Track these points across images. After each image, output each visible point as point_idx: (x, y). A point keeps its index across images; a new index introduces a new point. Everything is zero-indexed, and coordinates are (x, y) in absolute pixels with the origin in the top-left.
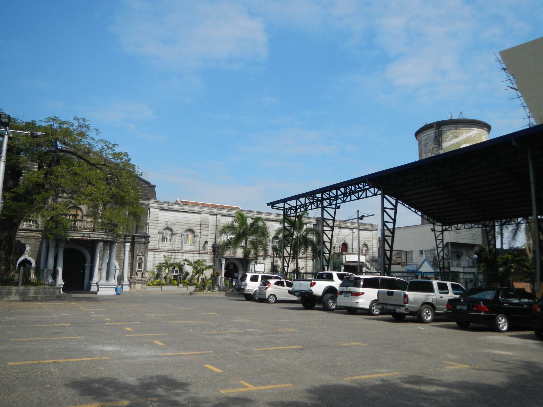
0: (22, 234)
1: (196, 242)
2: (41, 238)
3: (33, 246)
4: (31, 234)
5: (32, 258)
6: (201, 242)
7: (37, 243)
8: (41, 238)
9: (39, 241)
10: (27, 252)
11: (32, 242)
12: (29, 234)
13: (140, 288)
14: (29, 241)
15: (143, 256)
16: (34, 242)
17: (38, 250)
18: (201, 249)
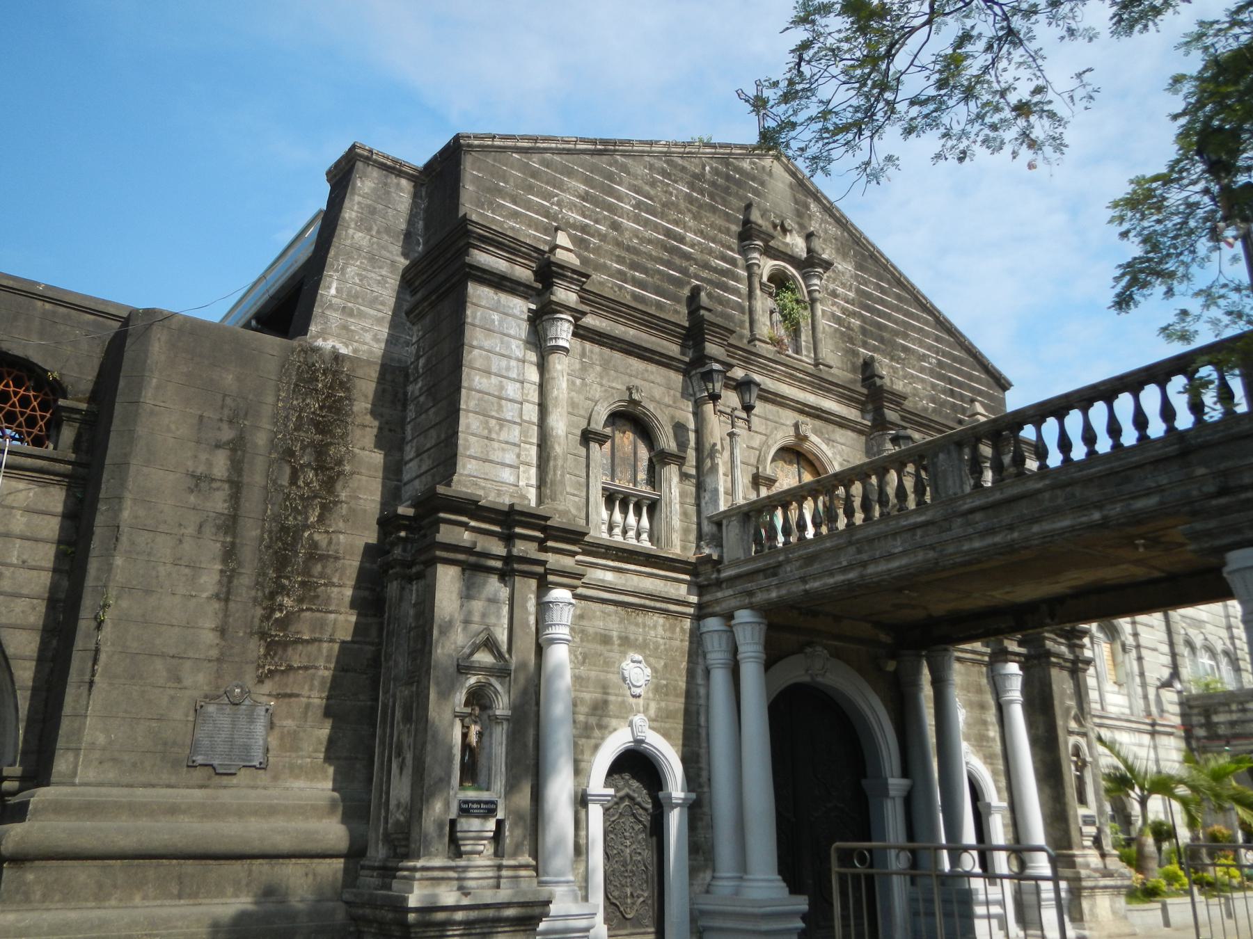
0: (609, 577)
1: (1129, 675)
2: (691, 610)
3: (662, 663)
4: (650, 585)
5: (666, 735)
6: (1148, 680)
7: (678, 643)
8: (691, 610)
9: (683, 630)
10: (639, 696)
11: (652, 633)
12: (635, 578)
13: (1110, 913)
14: (637, 625)
15: (1084, 735)
16: (660, 630)
17: (682, 685)
18: (1154, 710)
